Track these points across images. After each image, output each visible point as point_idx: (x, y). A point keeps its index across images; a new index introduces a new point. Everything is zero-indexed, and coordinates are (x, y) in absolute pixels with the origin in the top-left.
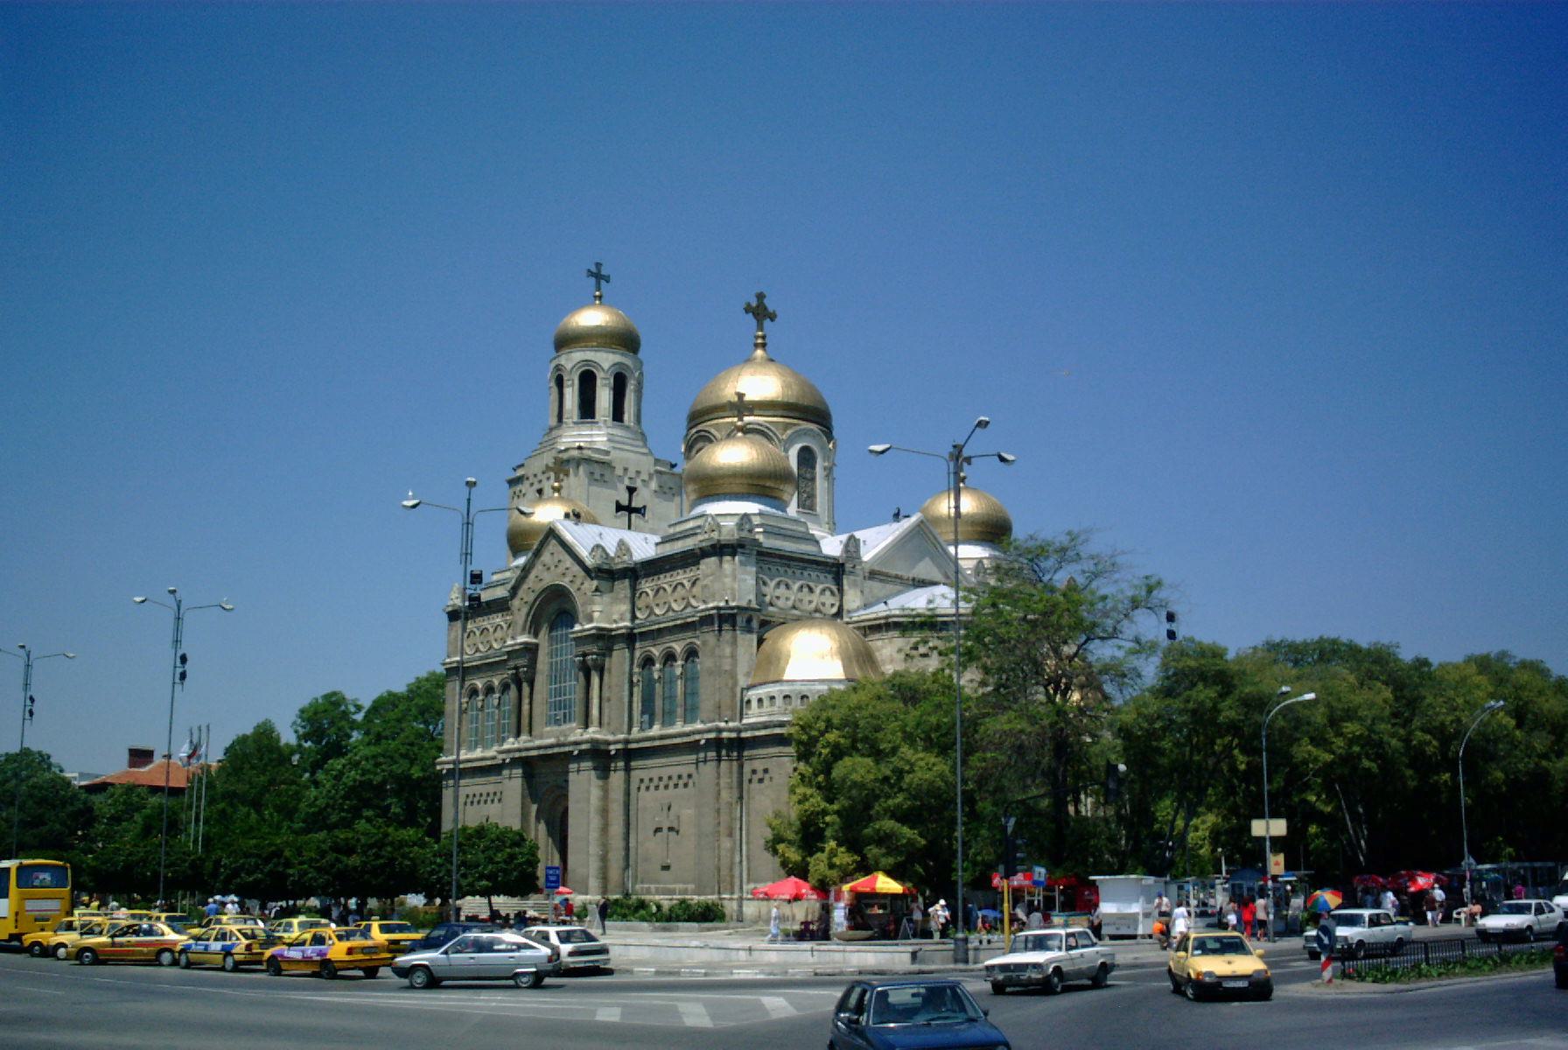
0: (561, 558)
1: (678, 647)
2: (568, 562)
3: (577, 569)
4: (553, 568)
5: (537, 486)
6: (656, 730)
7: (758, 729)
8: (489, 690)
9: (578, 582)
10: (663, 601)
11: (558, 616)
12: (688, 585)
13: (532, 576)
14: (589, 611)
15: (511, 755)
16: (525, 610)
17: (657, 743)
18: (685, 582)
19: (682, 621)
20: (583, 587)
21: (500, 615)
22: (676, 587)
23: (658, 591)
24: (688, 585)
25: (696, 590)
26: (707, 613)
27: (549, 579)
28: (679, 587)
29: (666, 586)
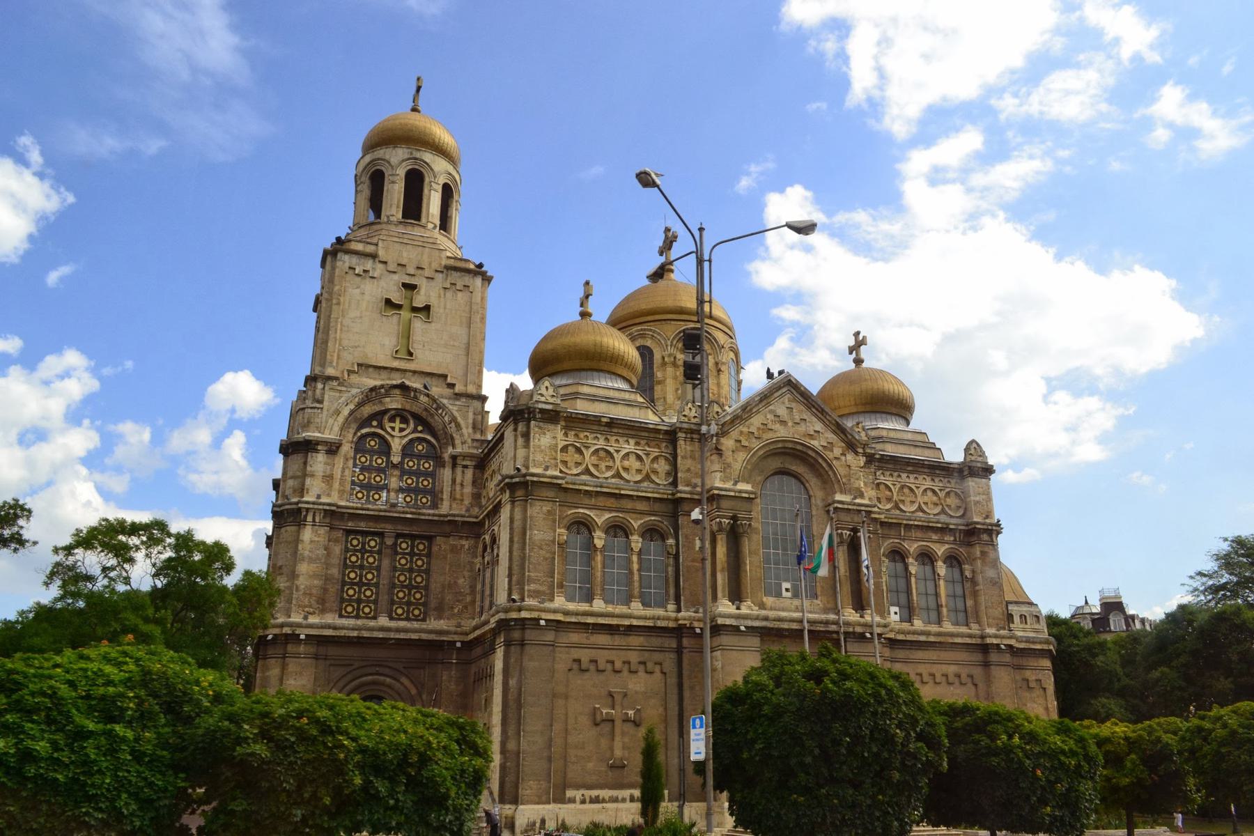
0: (805, 417)
1: (940, 550)
2: (819, 426)
3: (831, 436)
4: (790, 424)
5: (408, 280)
6: (918, 624)
7: (1034, 643)
8: (618, 529)
9: (837, 451)
10: (909, 499)
11: (772, 475)
12: (942, 495)
13: (756, 421)
14: (857, 485)
15: (750, 623)
16: (741, 456)
17: (932, 639)
18: (936, 489)
19: (945, 526)
20: (843, 458)
21: (632, 441)
22: (925, 490)
23: (902, 487)
24: (942, 495)
25: (949, 501)
26: (990, 527)
27: (782, 432)
28: (929, 493)
29: (913, 486)
